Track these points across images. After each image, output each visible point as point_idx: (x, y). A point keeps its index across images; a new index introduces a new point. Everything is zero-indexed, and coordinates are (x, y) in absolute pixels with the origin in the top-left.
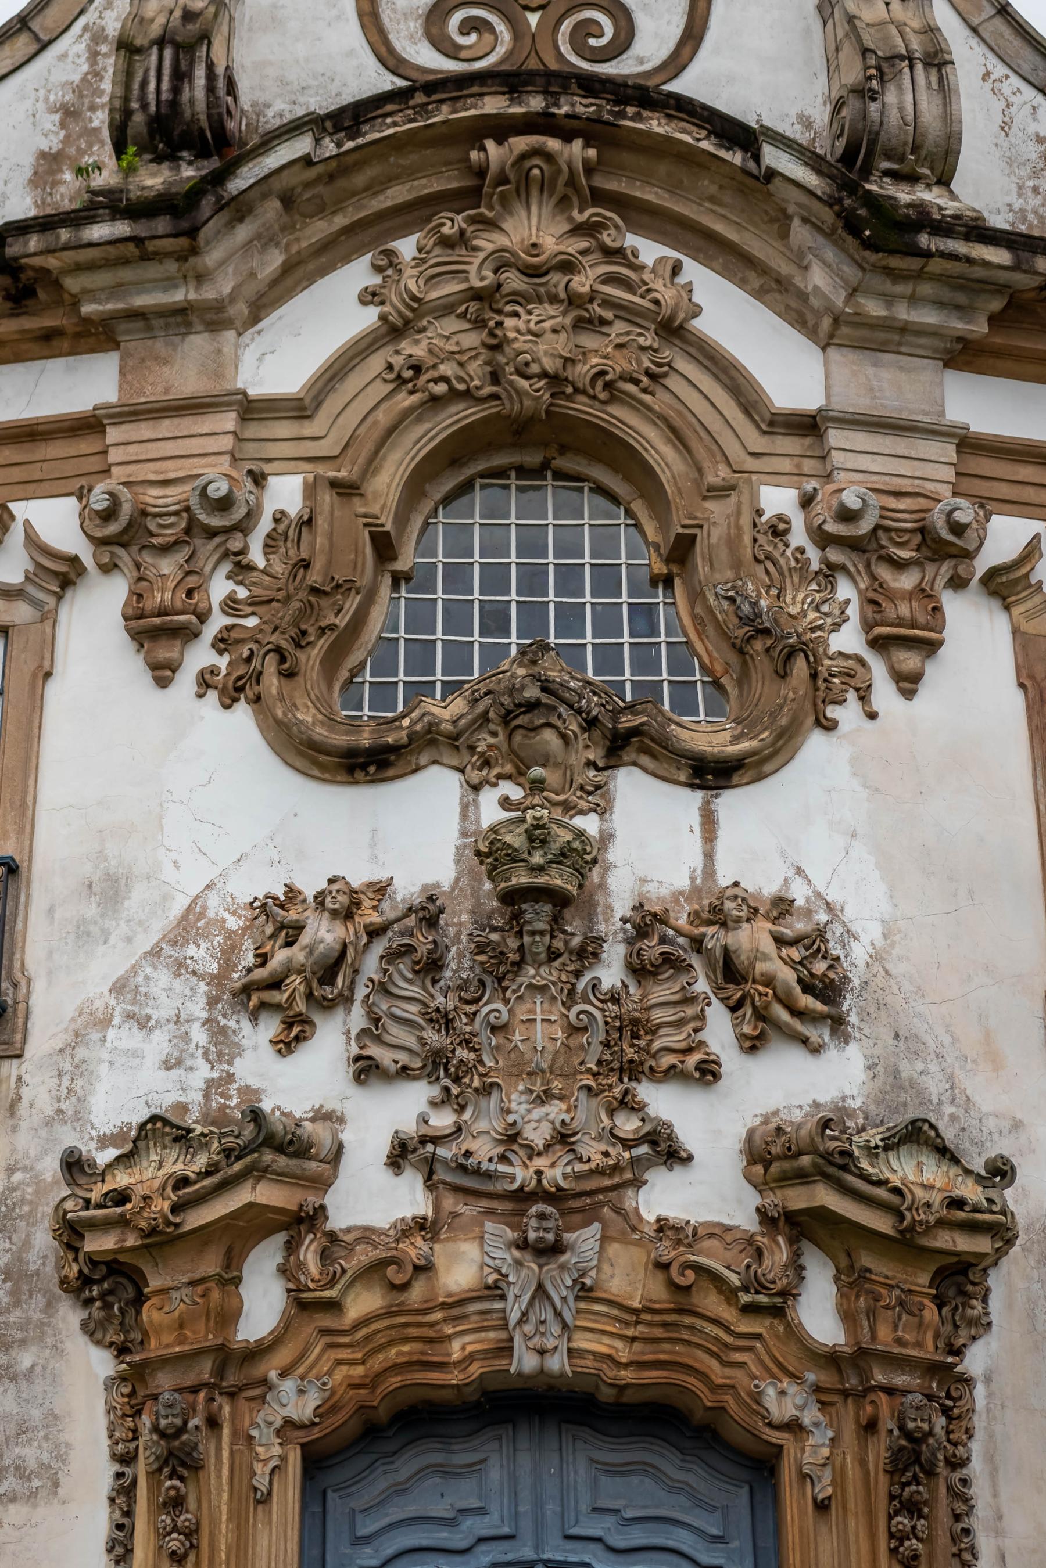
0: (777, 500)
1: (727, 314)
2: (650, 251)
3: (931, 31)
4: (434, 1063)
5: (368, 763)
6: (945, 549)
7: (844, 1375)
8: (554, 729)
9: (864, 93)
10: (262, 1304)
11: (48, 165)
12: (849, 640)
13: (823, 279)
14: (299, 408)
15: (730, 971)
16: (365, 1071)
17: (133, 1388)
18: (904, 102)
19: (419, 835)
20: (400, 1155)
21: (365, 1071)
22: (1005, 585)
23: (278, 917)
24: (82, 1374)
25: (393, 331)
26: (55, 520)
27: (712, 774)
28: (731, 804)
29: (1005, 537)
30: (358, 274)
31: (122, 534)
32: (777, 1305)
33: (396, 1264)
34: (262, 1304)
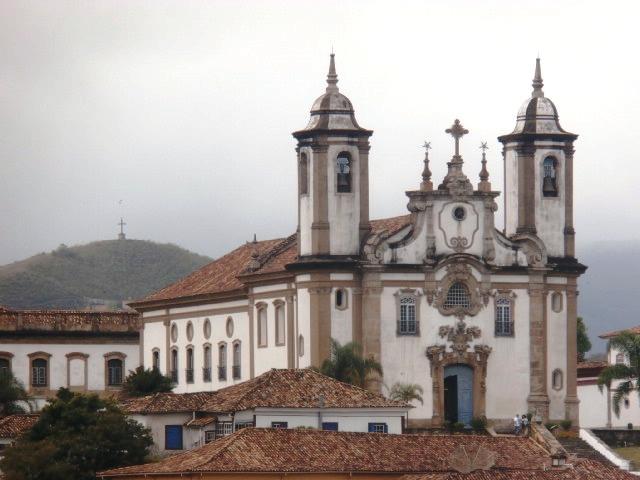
0: (478, 289)
1: (475, 272)
2: (469, 265)
3: (492, 244)
4: (454, 341)
5: (448, 315)
6: (489, 294)
7: (480, 363)
8: (460, 314)
9: (488, 253)
10: (441, 358)
11: (417, 253)
12: (482, 303)
13: (483, 269)
14: (440, 282)
15: (474, 333)
16: (448, 340)
17: (432, 364)
18: (491, 255)
19: (452, 322)
20: (451, 347)
21: (448, 340)
22: (494, 296)
23: (442, 329)
24: (426, 363)
25: (448, 275)
26: (420, 290)
27: (472, 316)
28: (474, 318)
29: (495, 290)
30: (445, 268)
31: (425, 293)
32: (475, 358)
33: (450, 355)
34: (441, 358)
